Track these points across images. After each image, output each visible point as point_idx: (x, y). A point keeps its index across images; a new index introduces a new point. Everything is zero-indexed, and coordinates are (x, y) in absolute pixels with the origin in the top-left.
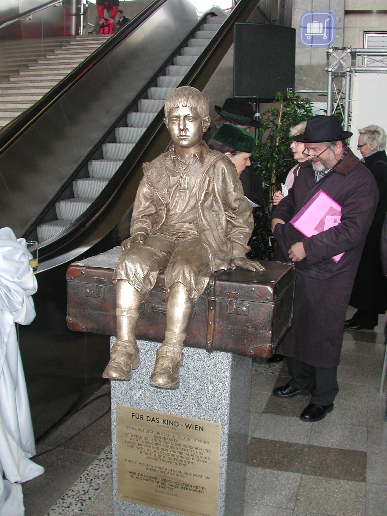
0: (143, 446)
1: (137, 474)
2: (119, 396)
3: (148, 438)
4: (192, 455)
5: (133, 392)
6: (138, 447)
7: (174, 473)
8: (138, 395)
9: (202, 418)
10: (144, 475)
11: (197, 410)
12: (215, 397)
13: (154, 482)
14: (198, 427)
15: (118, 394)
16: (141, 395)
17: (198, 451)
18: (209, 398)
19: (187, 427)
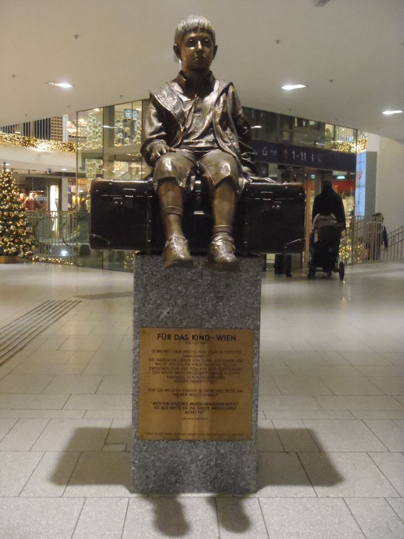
3: (175, 360)
5: (159, 310)
8: (165, 313)
9: (234, 327)
12: (247, 302)
16: (168, 313)
19: (218, 339)
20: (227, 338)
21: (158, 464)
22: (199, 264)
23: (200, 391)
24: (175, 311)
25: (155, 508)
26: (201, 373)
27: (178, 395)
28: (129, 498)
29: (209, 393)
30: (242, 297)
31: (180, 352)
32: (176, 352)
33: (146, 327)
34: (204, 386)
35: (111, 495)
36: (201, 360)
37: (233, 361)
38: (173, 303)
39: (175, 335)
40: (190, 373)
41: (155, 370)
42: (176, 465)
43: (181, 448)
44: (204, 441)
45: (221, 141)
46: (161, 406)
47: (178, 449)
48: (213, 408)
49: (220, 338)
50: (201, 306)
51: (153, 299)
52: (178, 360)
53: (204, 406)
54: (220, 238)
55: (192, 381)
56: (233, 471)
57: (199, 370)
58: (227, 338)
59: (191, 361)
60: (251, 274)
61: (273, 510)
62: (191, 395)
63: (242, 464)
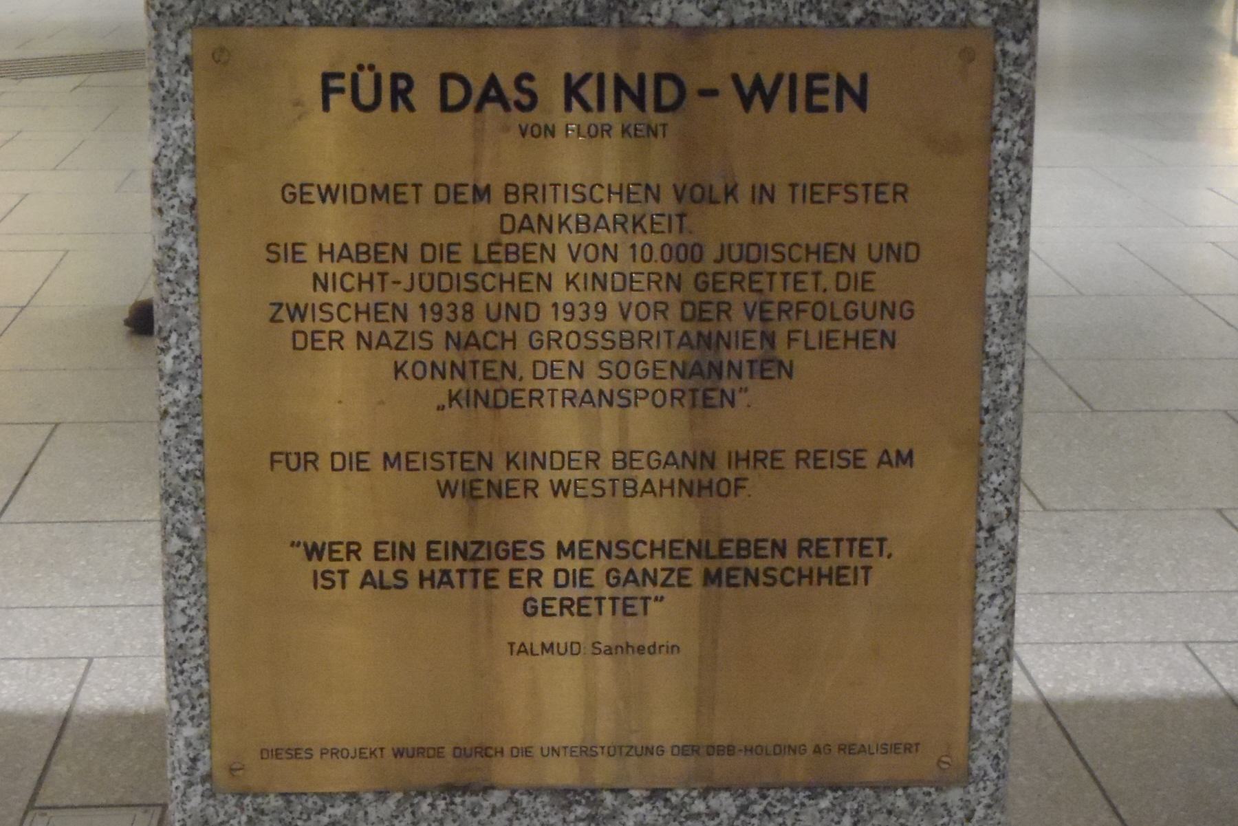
0: (414, 313)
1: (367, 552)
3: (450, 252)
6: (377, 329)
7: (656, 476)
10: (421, 552)
14: (831, 84)
17: (829, 271)
19: (747, 103)
20: (810, 92)
23: (626, 459)
26: (630, 340)
27: (471, 492)
29: (688, 474)
31: (481, 194)
32: (452, 195)
33: (237, 21)
34: (652, 428)
36: (624, 254)
37: (849, 252)
39: (445, 78)
40: (554, 340)
41: (308, 326)
44: (655, 794)
46: (356, 570)
48: (710, 578)
49: (756, 94)
52: (466, 253)
55: (571, 398)
57: (614, 321)
58: (810, 92)
59: (562, 255)
62: (560, 489)
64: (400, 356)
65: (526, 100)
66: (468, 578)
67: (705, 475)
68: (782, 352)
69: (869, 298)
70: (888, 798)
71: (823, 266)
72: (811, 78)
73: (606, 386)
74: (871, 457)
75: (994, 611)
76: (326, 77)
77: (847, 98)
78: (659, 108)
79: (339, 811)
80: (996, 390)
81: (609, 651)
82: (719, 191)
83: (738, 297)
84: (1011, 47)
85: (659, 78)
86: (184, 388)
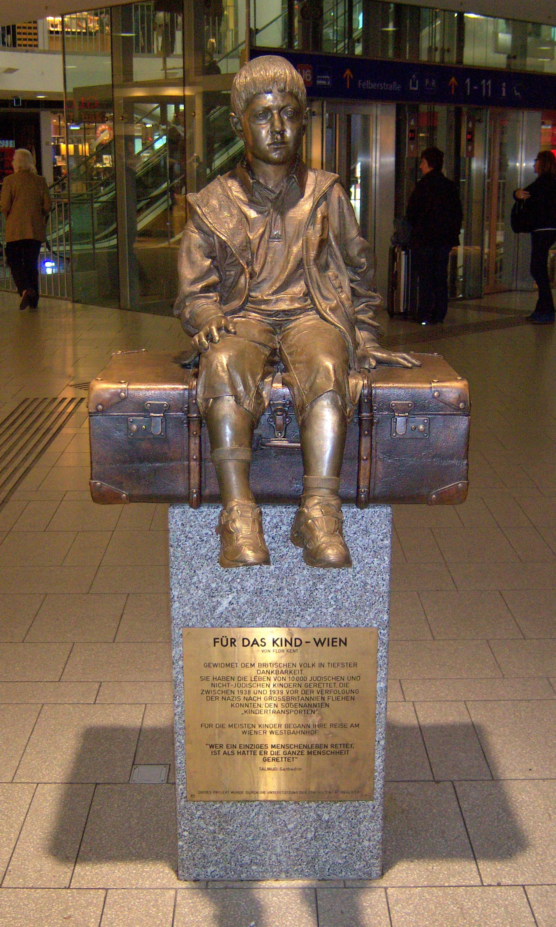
0: (236, 693)
1: (225, 746)
2: (188, 611)
4: (327, 692)
5: (214, 600)
8: (225, 603)
9: (344, 624)
10: (238, 746)
11: (335, 612)
12: (366, 584)
13: (258, 753)
14: (338, 640)
15: (187, 608)
16: (231, 603)
18: (356, 588)
21: (221, 836)
22: (281, 521)
24: (242, 600)
25: (217, 913)
28: (176, 890)
29: (303, 729)
30: (358, 576)
31: (253, 665)
35: (147, 884)
36: (287, 679)
38: (239, 587)
39: (243, 639)
42: (250, 838)
43: (258, 814)
45: (318, 295)
47: (254, 814)
48: (309, 753)
50: (286, 591)
51: (204, 581)
53: (296, 749)
54: (316, 501)
55: (274, 712)
56: (343, 846)
60: (373, 536)
61: (409, 914)
62: (272, 732)
63: (359, 836)
64: (233, 702)
65: (263, 644)
66: (249, 753)
67: (307, 729)
68: (326, 701)
69: (348, 689)
70: (354, 803)
71: (336, 682)
72: (333, 639)
73: (283, 709)
74: (349, 725)
75: (380, 760)
76: (215, 639)
77: (342, 644)
78: (296, 646)
79: (218, 805)
80: (380, 710)
81: (284, 770)
82: (310, 665)
83: (315, 689)
84: (382, 631)
85: (295, 639)
86: (180, 708)
